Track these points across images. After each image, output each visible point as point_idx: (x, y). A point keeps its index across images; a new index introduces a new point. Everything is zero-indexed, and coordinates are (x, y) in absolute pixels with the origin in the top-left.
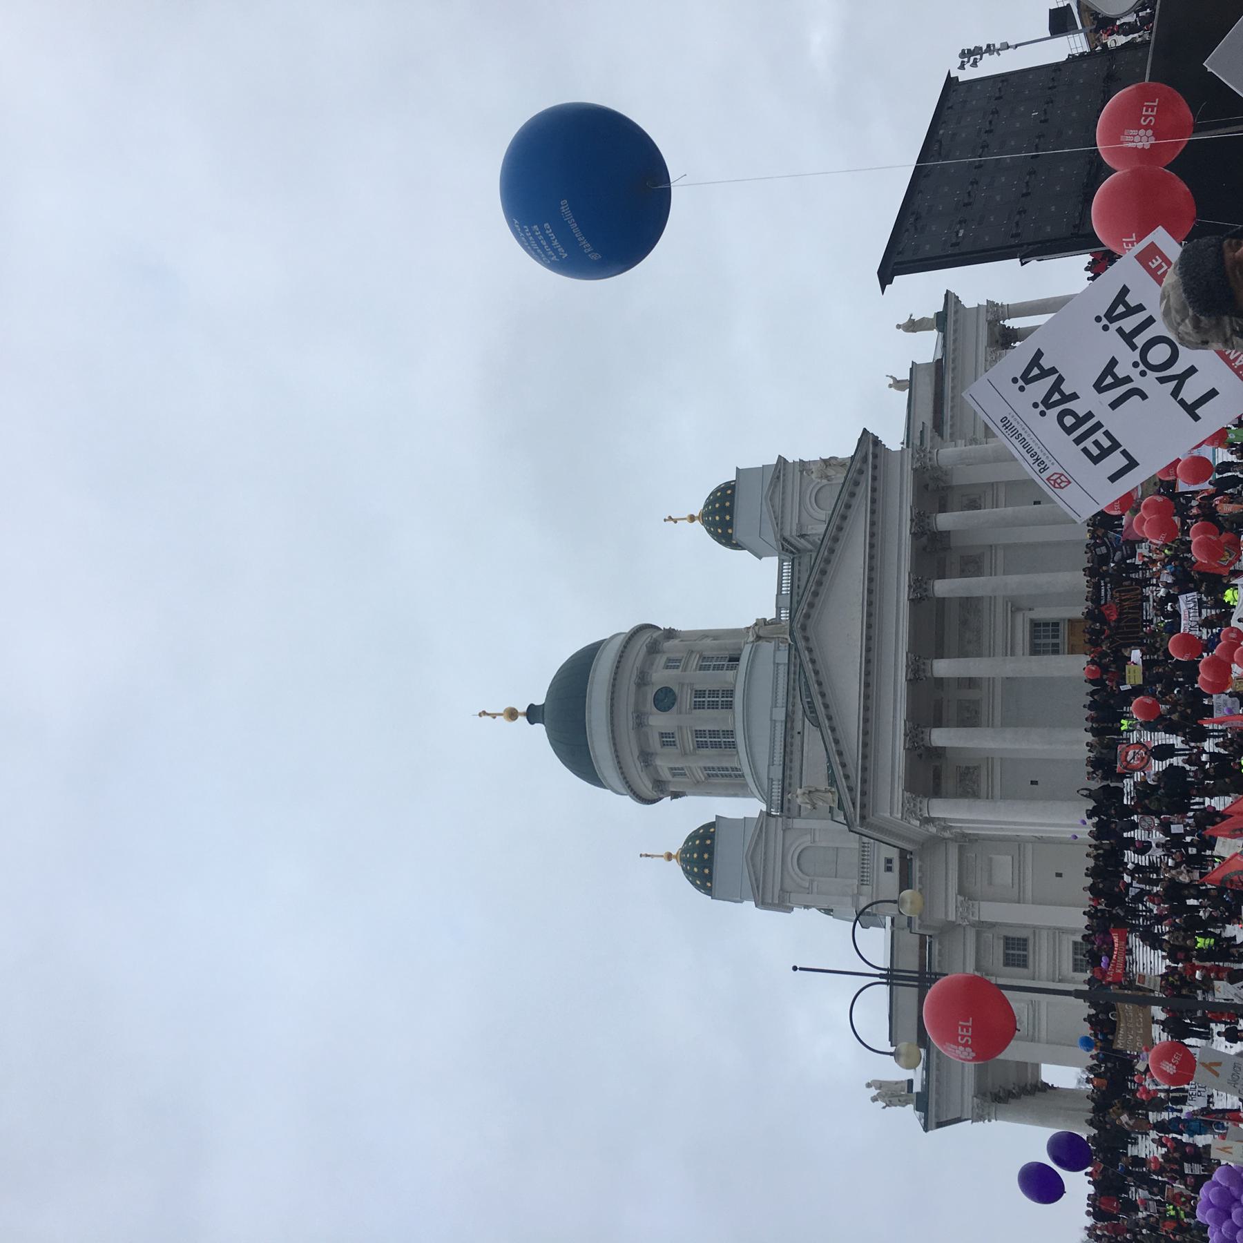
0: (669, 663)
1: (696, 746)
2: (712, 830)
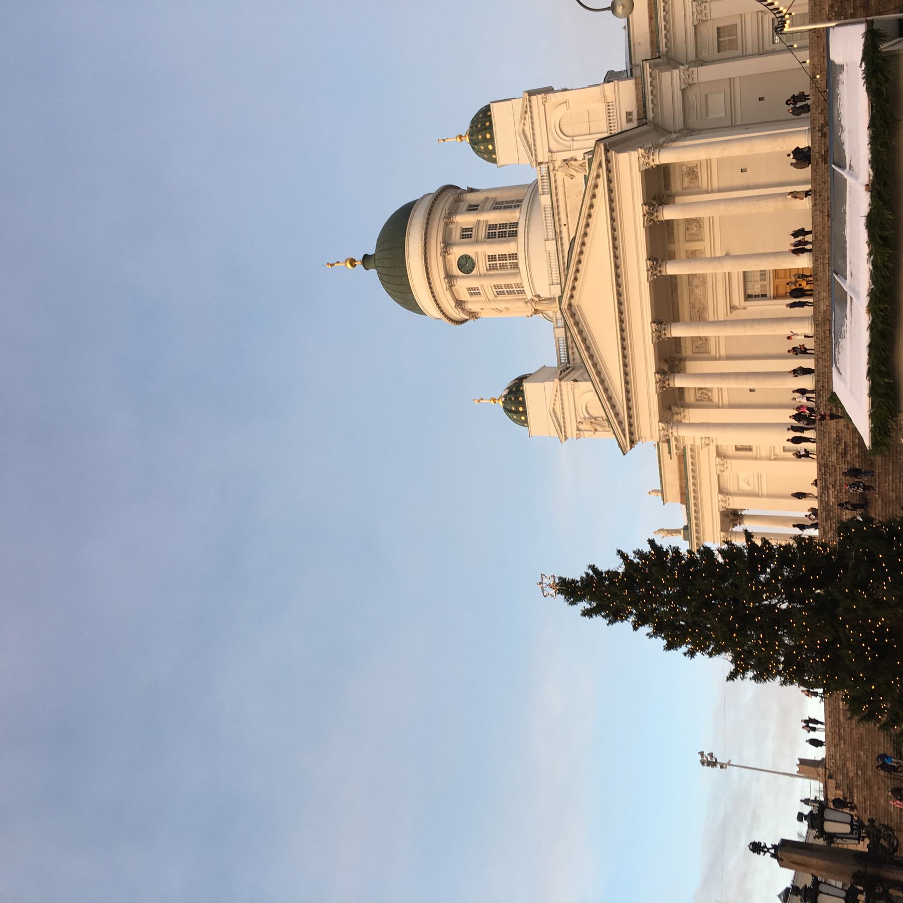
0: (463, 232)
1: (496, 294)
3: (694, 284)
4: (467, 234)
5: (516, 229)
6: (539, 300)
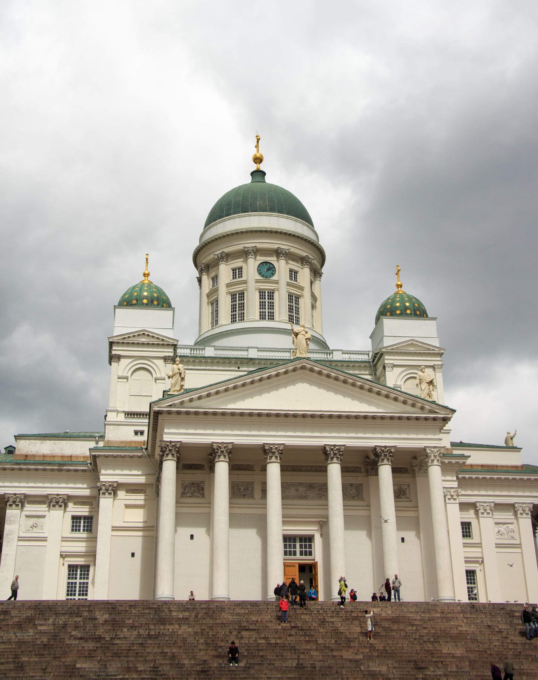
0: (294, 273)
1: (233, 294)
2: (165, 305)
3: (299, 488)
4: (293, 274)
5: (295, 323)
6: (306, 339)
